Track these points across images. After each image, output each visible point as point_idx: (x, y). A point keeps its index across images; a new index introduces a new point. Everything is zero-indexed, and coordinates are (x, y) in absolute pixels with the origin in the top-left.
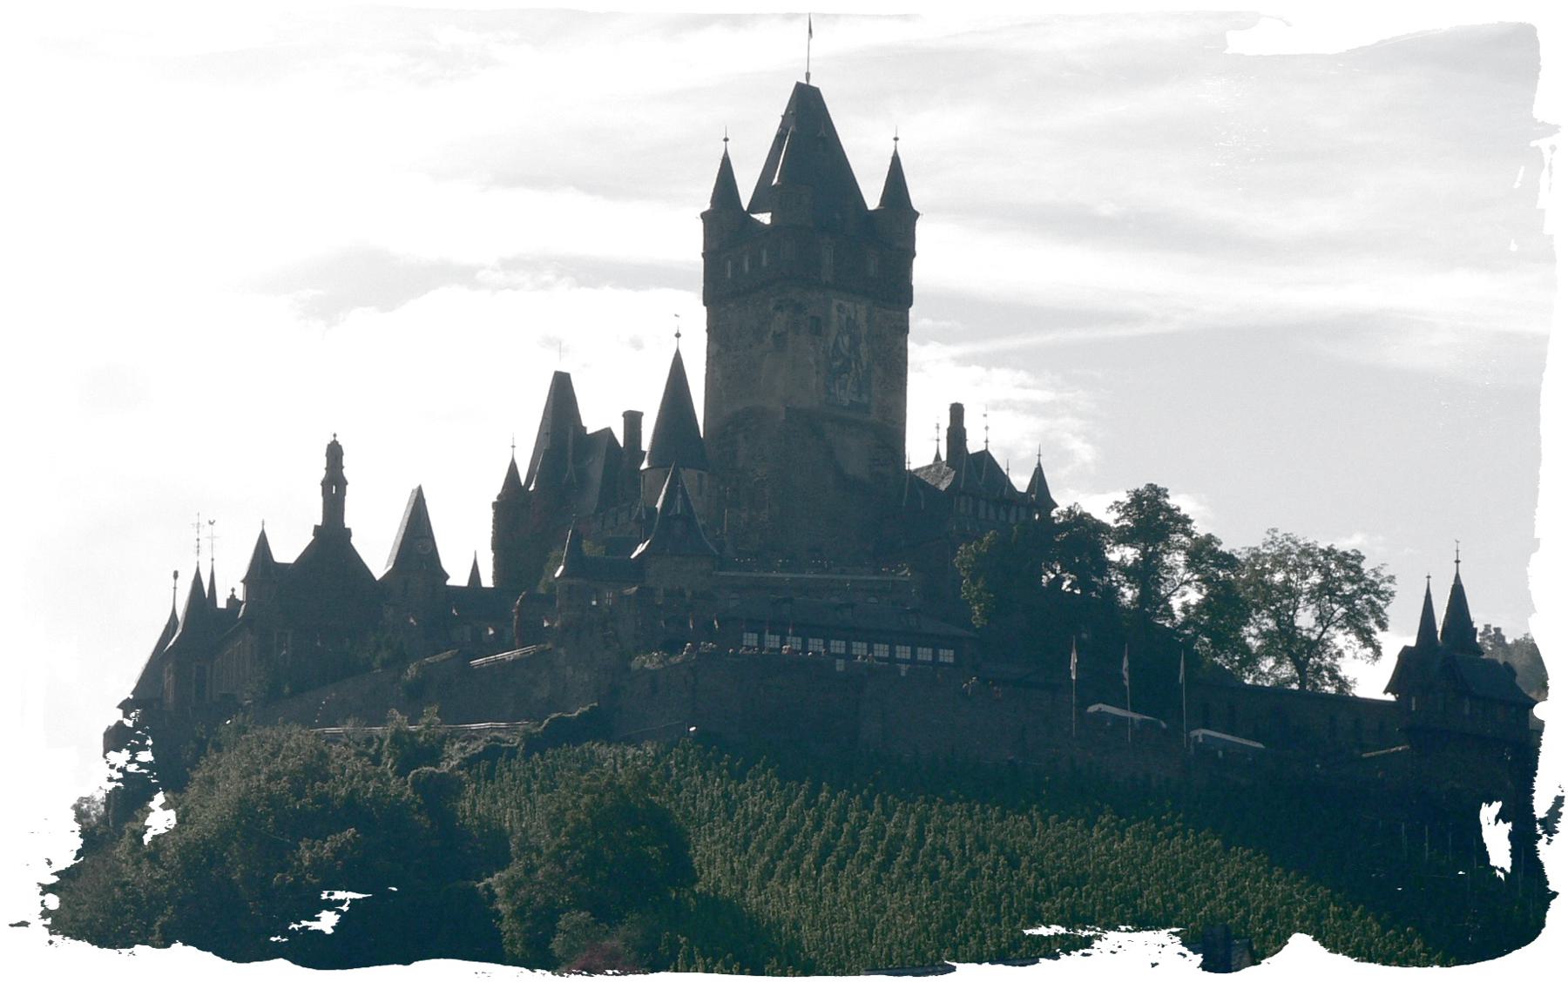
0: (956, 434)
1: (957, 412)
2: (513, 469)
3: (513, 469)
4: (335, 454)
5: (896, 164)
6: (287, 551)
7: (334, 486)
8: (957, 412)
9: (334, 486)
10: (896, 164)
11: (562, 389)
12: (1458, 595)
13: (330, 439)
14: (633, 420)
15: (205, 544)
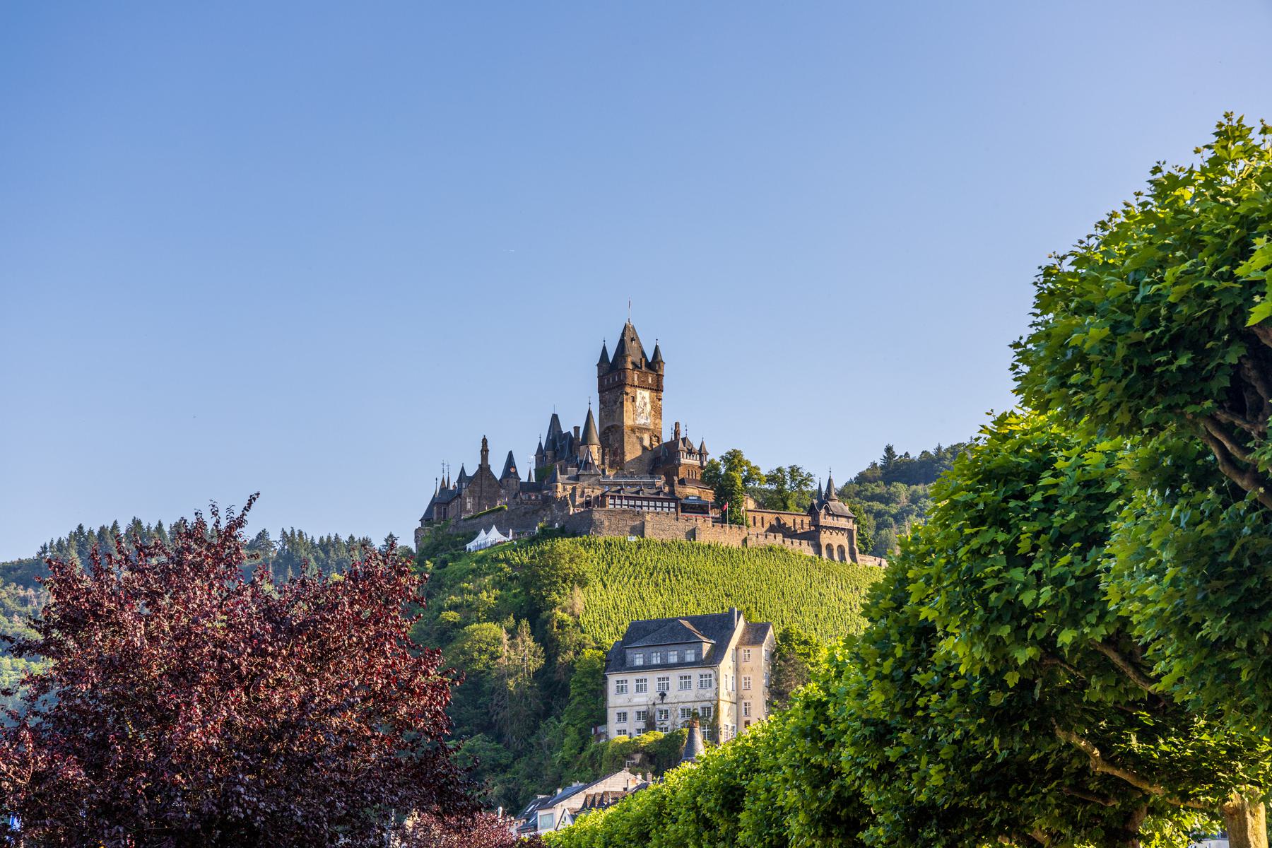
0: (677, 433)
1: (677, 424)
2: (540, 444)
3: (540, 444)
4: (485, 442)
5: (657, 347)
6: (470, 472)
7: (485, 451)
8: (677, 424)
9: (485, 451)
10: (657, 347)
11: (555, 417)
12: (830, 480)
13: (483, 437)
14: (577, 429)
15: (446, 468)
